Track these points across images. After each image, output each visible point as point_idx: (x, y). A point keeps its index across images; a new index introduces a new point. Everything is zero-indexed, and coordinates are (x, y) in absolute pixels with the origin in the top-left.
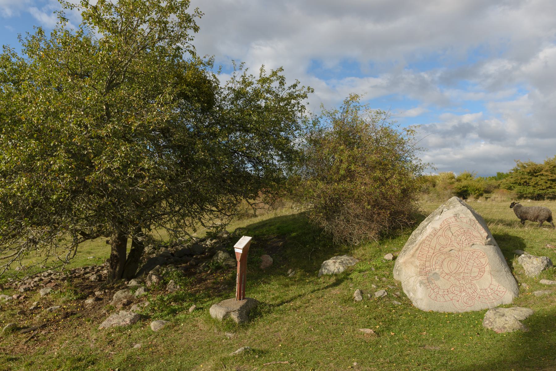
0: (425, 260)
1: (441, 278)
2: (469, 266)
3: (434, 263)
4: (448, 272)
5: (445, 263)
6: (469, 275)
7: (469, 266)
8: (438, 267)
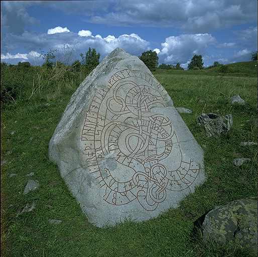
0: (92, 138)
1: (119, 165)
2: (153, 140)
3: (106, 142)
4: (127, 153)
6: (154, 152)
8: (113, 147)
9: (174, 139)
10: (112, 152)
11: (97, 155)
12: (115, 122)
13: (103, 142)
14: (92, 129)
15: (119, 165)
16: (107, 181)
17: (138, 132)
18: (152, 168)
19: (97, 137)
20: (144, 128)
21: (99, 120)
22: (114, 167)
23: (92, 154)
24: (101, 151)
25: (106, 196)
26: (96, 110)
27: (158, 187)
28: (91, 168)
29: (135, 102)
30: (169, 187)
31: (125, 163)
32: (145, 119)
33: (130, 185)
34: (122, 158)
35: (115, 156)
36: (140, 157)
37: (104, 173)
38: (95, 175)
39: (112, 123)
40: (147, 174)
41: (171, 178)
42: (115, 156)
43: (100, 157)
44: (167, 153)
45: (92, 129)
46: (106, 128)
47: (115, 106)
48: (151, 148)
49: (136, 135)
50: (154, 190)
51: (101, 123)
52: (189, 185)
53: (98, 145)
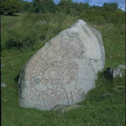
2: (63, 75)
5: (48, 71)
7: (63, 75)
8: (41, 74)
10: (40, 76)
12: (48, 63)
13: (37, 71)
16: (33, 89)
24: (35, 75)
27: (56, 98)
28: (27, 81)
29: (63, 53)
30: (63, 99)
31: (44, 83)
33: (43, 93)
34: (44, 80)
35: (41, 78)
37: (32, 85)
41: (65, 96)
42: (41, 78)
46: (41, 64)
48: (61, 78)
50: (54, 99)
51: (40, 61)
52: (74, 101)
53: (34, 71)
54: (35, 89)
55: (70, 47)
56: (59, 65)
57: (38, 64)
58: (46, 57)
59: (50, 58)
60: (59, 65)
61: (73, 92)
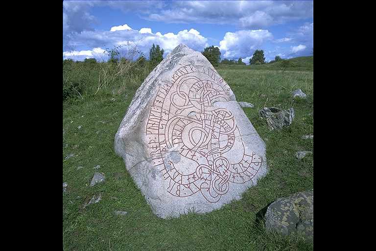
0: (157, 132)
1: (183, 158)
2: (215, 134)
3: (170, 136)
4: (191, 146)
5: (185, 134)
6: (217, 146)
9: (237, 133)
10: (176, 146)
11: (161, 149)
14: (156, 123)
15: (183, 158)
16: (171, 174)
17: (201, 126)
18: (215, 161)
19: (161, 131)
20: (207, 122)
21: (163, 115)
22: (178, 160)
23: (157, 147)
24: (165, 145)
25: (170, 189)
26: (161, 105)
27: (221, 179)
28: (155, 161)
29: (198, 96)
30: (231, 179)
31: (189, 156)
32: (208, 113)
36: (203, 151)
38: (159, 168)
39: (175, 117)
40: (210, 166)
41: (234, 171)
43: (164, 150)
44: (229, 146)
45: (156, 123)
46: (170, 122)
47: (179, 101)
48: (213, 141)
49: (199, 128)
50: (217, 183)
51: (165, 117)
53: (162, 138)
54: (177, 174)
55: (205, 84)
56: (201, 117)
57: (164, 122)
58: (172, 107)
59: (181, 108)
60: (201, 117)
61: (243, 162)
